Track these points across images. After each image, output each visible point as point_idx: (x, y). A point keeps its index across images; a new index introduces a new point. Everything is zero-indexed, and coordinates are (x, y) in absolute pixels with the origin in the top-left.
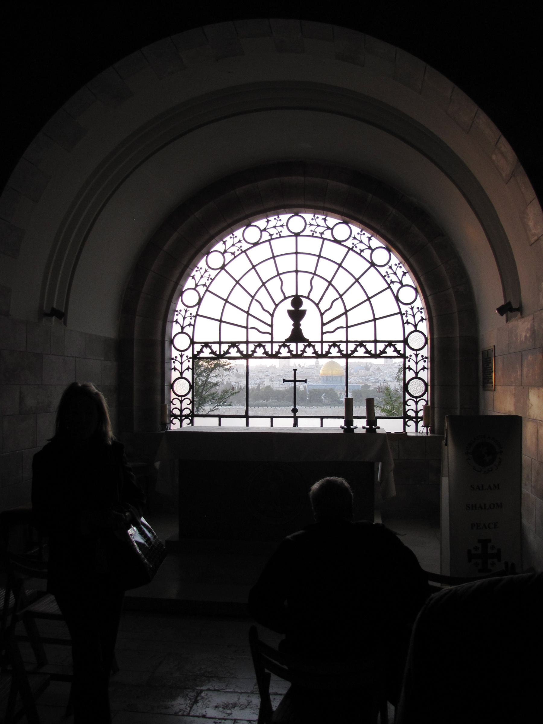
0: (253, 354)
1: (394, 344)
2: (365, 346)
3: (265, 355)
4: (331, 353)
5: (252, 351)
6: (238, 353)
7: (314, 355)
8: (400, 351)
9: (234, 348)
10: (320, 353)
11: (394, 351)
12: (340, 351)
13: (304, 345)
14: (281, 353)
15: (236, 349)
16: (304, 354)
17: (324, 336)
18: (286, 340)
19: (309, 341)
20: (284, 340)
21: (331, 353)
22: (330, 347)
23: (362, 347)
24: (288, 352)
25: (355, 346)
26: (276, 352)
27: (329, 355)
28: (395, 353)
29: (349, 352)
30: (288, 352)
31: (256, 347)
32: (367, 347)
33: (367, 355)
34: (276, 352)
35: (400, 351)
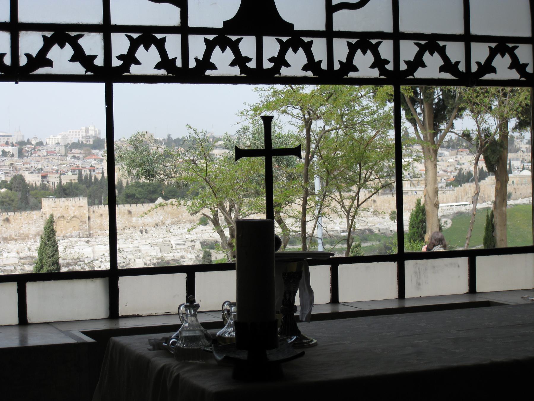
0: (125, 67)
1: (510, 45)
2: (442, 52)
3: (162, 72)
4: (355, 69)
5: (120, 57)
6: (78, 63)
7: (310, 74)
8: (526, 65)
9: (62, 46)
10: (324, 66)
11: (511, 68)
12: (379, 63)
13: (280, 41)
14: (213, 67)
15: (68, 50)
16: (281, 71)
17: (336, 16)
18: (225, 23)
19: (296, 28)
20: (221, 26)
21: (355, 69)
22: (352, 49)
23: (436, 54)
24: (232, 64)
25: (417, 49)
26: (196, 60)
27: (352, 75)
28: (514, 71)
29: (403, 67)
30: (232, 64)
31: (134, 45)
32: (449, 52)
33: (447, 76)
34: (196, 60)
35: (526, 65)
